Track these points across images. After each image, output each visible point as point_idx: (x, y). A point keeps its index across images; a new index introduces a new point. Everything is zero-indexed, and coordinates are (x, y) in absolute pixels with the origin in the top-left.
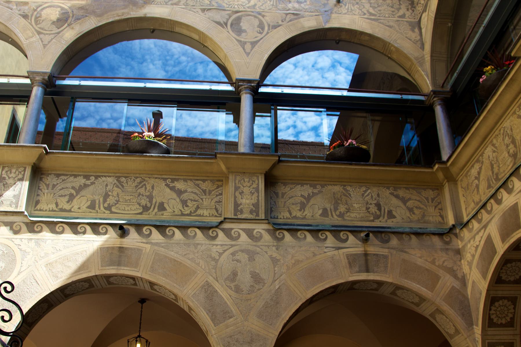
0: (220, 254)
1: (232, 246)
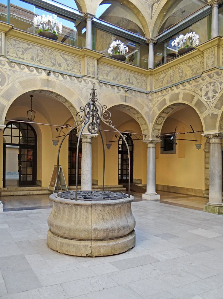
0: (83, 88)
1: (86, 86)
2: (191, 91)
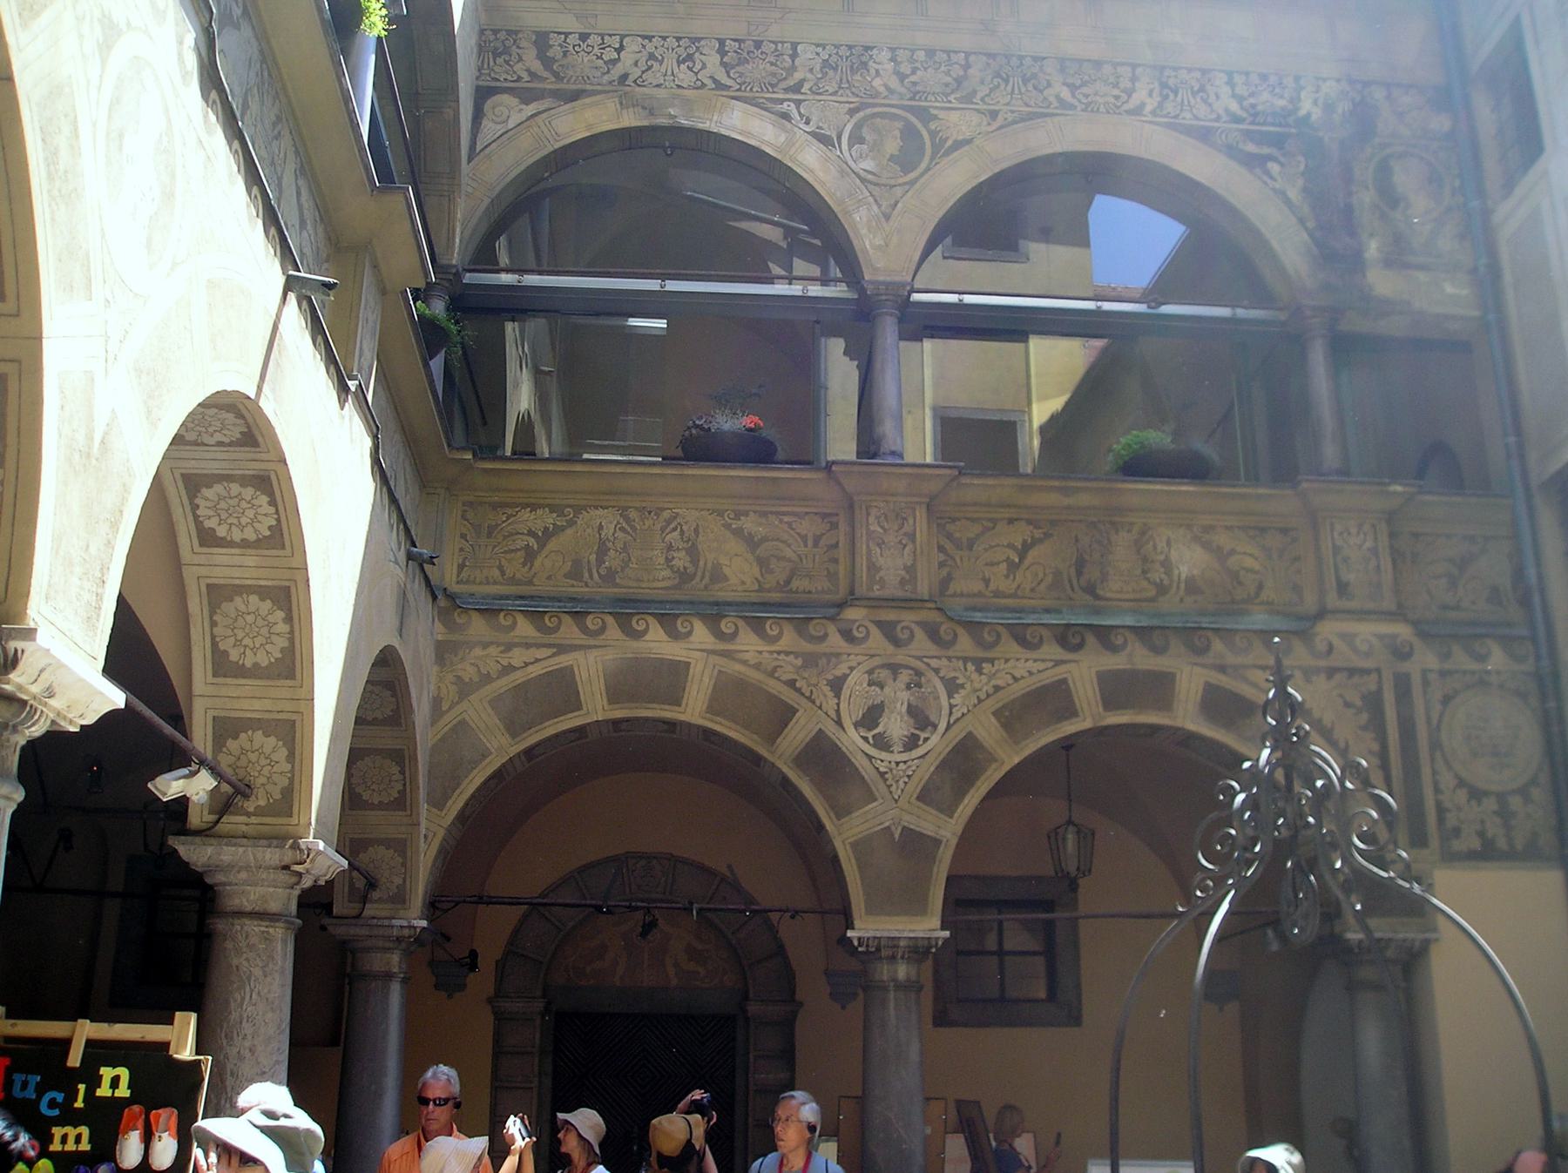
2: (771, 674)
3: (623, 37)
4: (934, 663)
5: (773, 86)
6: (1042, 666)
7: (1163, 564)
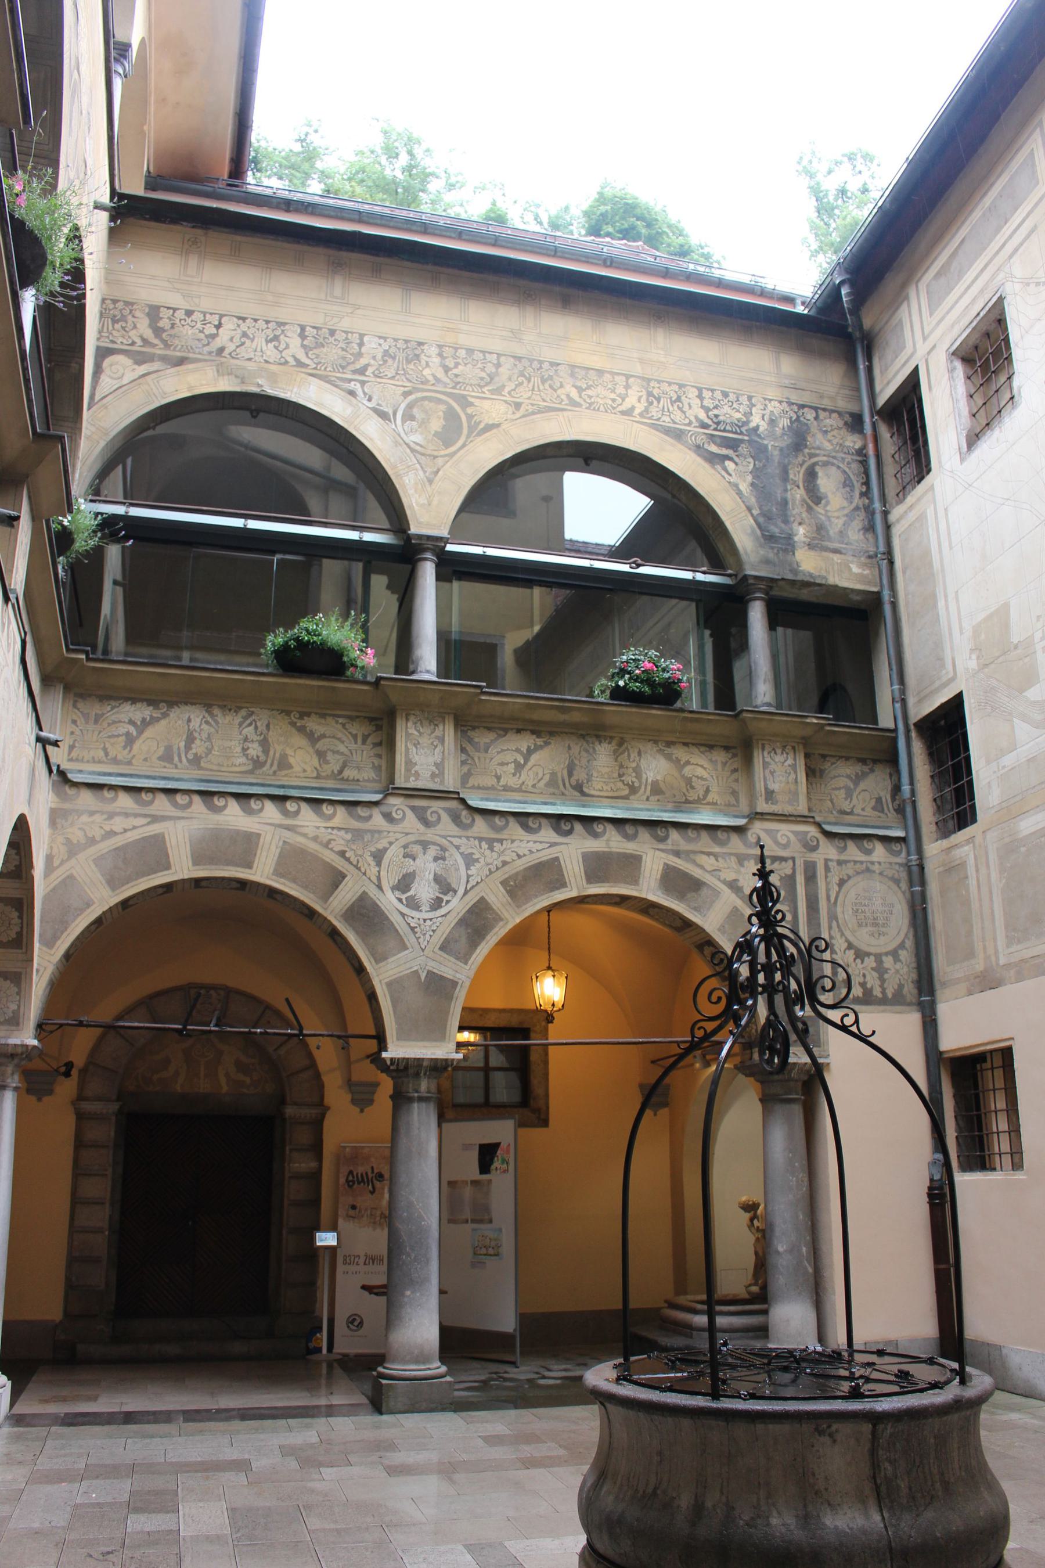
2: (327, 845)
3: (221, 316)
4: (456, 841)
5: (343, 368)
6: (540, 846)
7: (635, 770)
